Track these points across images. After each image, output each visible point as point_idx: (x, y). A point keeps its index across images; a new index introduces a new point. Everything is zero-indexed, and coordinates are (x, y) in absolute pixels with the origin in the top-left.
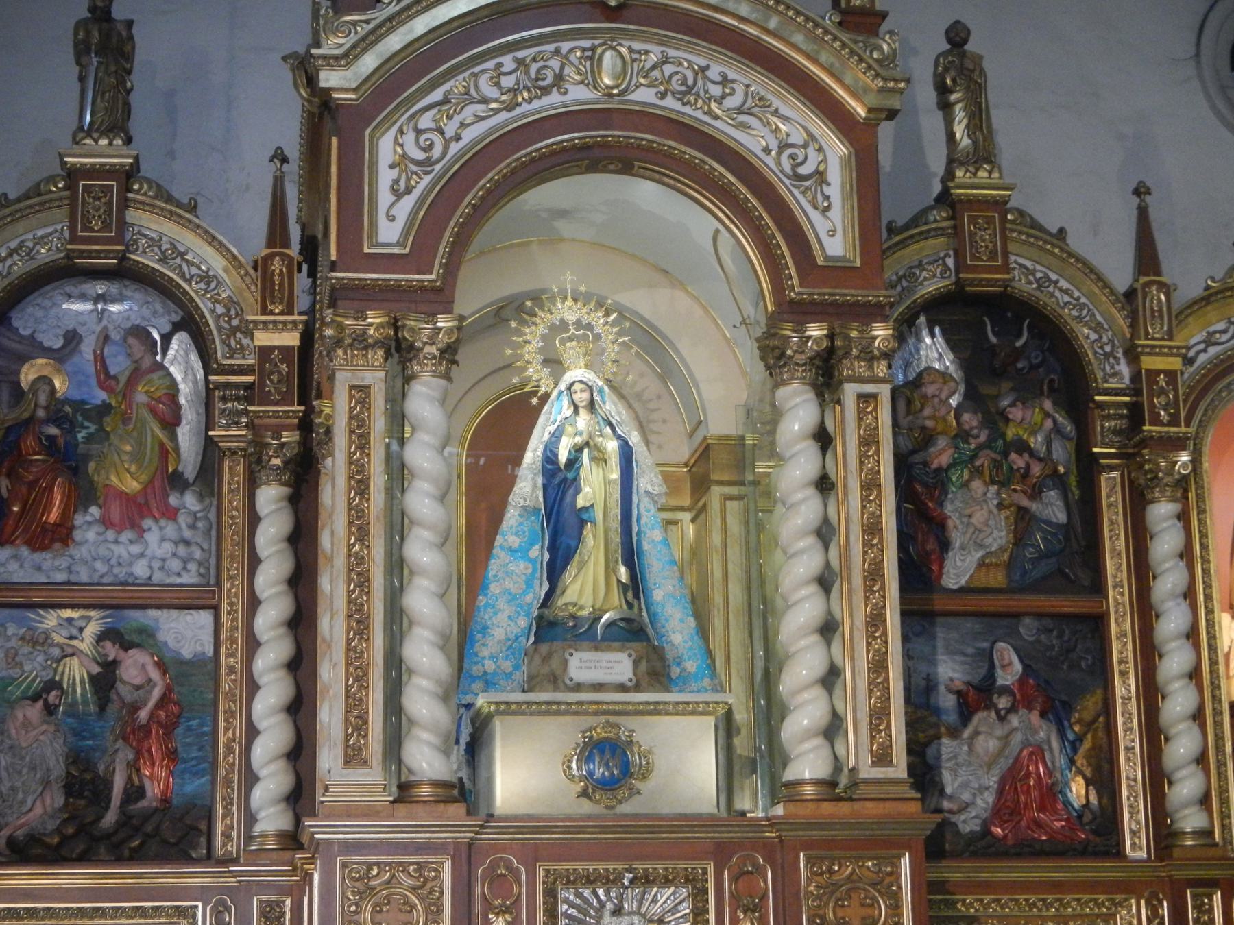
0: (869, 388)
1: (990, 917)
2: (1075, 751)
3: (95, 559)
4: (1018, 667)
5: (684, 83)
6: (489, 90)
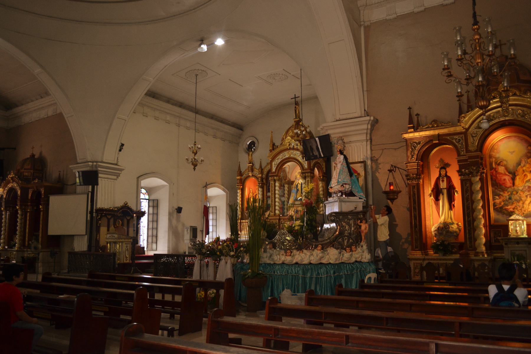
6: (281, 157)
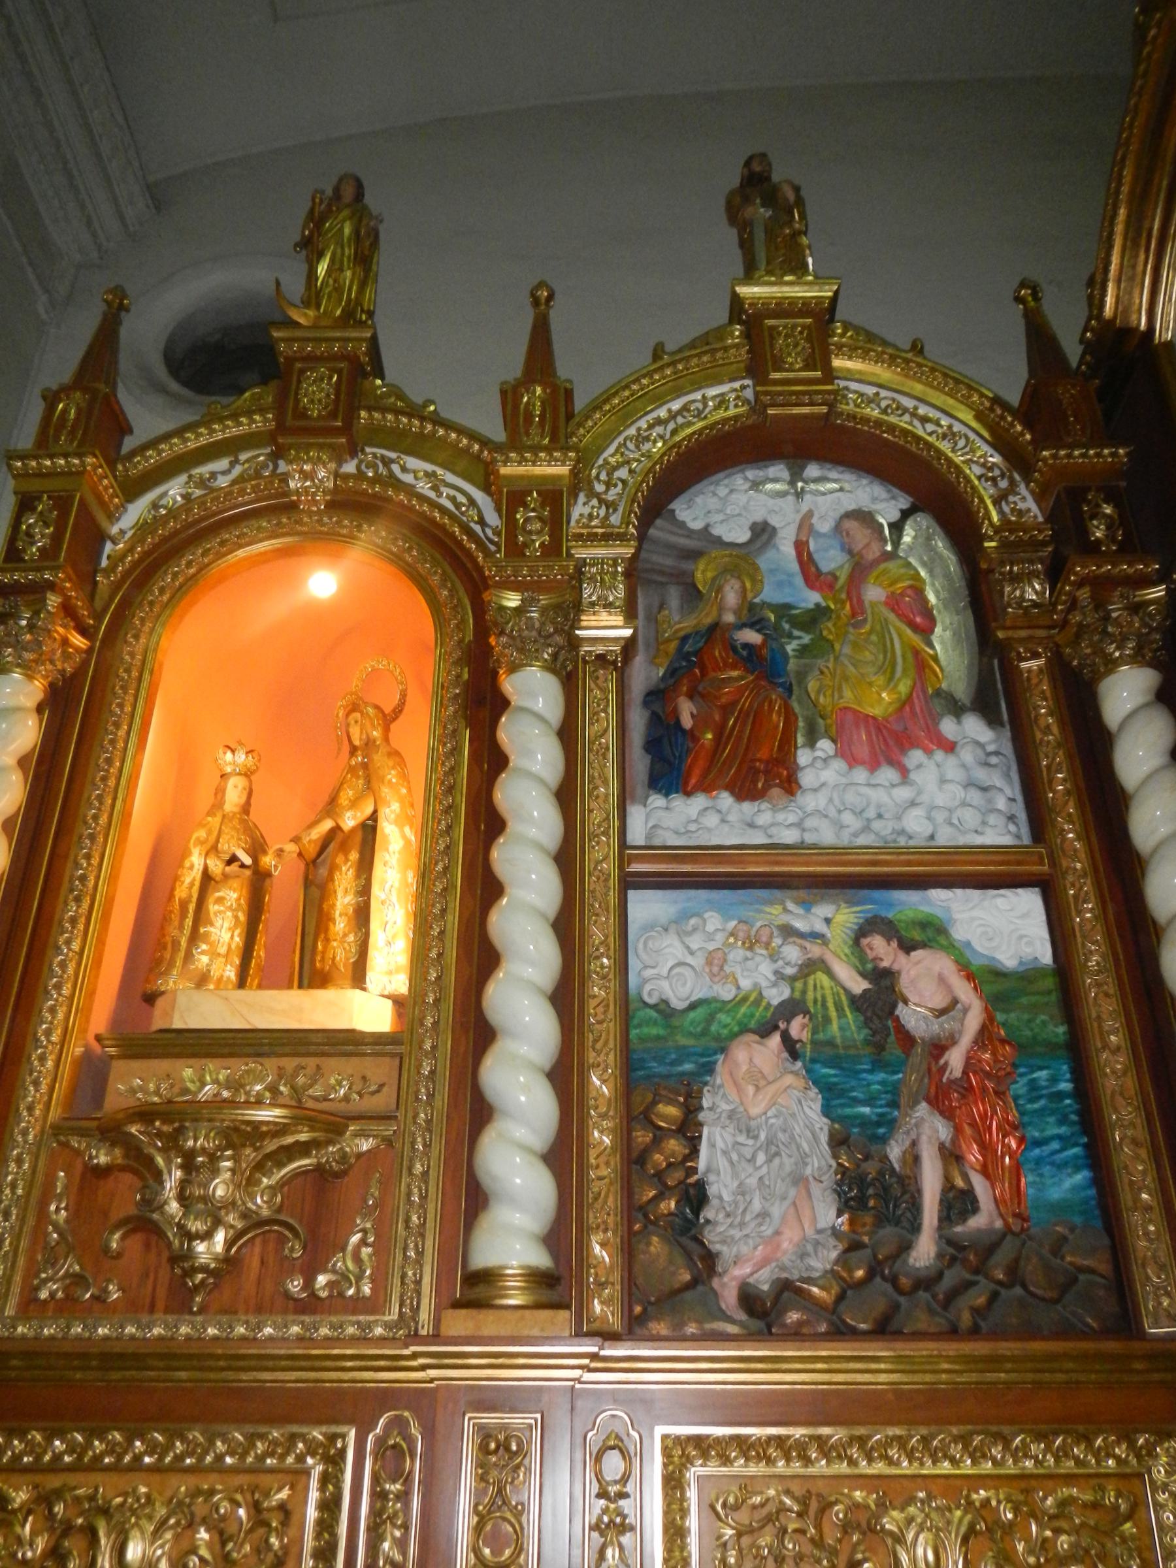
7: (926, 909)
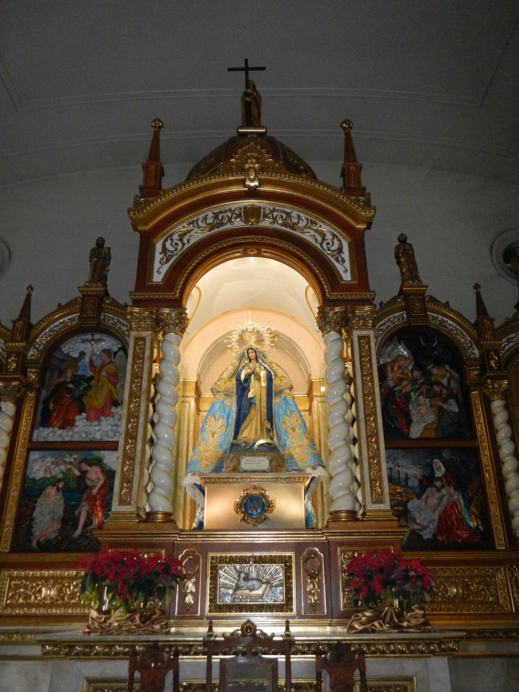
0: (364, 333)
1: (439, 577)
2: (470, 504)
3: (81, 432)
4: (443, 469)
5: (282, 217)
7: (98, 455)
